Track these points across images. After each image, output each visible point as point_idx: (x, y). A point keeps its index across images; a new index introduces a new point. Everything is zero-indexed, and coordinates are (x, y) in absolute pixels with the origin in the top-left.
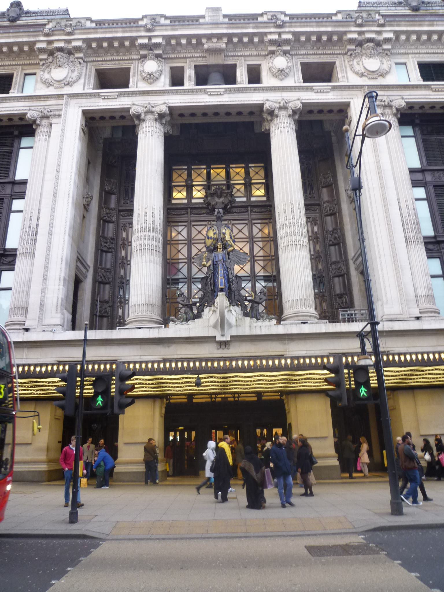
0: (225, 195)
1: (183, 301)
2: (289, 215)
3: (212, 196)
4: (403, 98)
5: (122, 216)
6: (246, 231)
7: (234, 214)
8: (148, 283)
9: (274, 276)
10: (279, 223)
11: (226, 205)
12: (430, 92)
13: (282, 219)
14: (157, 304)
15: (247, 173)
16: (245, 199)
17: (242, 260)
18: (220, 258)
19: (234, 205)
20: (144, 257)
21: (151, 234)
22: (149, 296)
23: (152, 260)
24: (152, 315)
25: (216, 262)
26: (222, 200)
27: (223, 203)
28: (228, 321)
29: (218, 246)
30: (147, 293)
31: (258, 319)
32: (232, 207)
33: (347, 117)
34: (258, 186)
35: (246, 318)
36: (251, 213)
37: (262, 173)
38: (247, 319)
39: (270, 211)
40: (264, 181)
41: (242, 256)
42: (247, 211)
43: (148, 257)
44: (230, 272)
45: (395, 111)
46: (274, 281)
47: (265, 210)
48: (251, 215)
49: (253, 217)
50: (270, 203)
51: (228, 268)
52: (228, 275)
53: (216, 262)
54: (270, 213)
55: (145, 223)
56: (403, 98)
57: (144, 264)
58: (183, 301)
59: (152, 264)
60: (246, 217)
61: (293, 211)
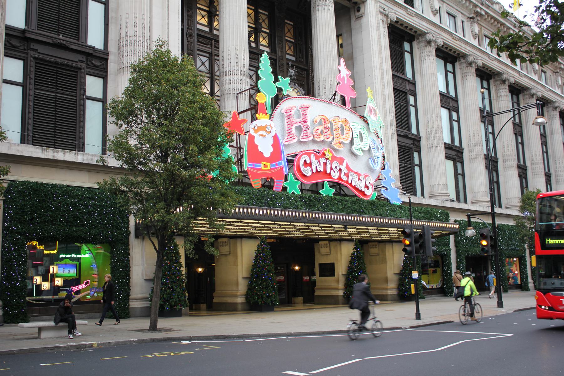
4: (395, 13)
12: (405, 13)
33: (359, 10)
45: (389, 22)
56: (395, 13)
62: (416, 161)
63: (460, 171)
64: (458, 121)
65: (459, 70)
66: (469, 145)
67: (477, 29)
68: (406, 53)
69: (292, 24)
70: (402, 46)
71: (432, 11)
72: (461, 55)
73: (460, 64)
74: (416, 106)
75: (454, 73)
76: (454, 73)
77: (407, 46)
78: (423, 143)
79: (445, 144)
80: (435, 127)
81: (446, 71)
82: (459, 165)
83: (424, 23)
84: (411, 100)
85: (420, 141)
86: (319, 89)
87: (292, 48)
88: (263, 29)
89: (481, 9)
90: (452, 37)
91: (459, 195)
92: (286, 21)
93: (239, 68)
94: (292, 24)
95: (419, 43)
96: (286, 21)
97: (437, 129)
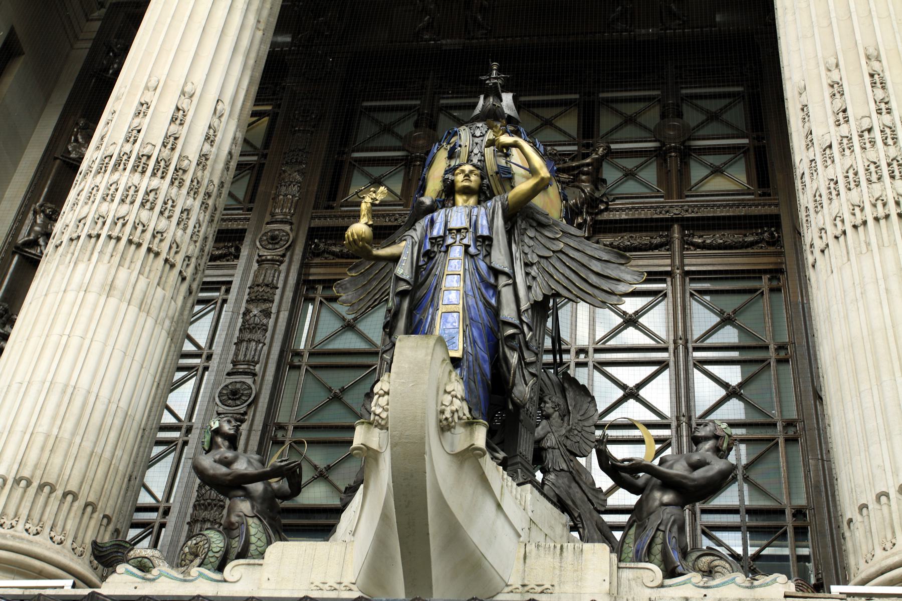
2: (860, 102)
6: (657, 320)
8: (61, 379)
9: (799, 513)
10: (810, 145)
13: (824, 128)
14: (88, 494)
17: (593, 279)
19: (606, 216)
20: (81, 267)
21: (145, 182)
22: (52, 445)
23: (120, 283)
24: (43, 539)
28: (455, 534)
30: (43, 427)
31: (671, 572)
35: (587, 546)
36: (683, 249)
37: (737, 115)
38: (598, 555)
39: (775, 242)
40: (746, 141)
41: (597, 266)
42: (666, 244)
43: (102, 268)
44: (507, 294)
46: (801, 533)
47: (750, 239)
48: (682, 257)
49: (694, 264)
50: (773, 210)
51: (496, 273)
52: (494, 312)
53: (434, 241)
54: (771, 249)
57: (70, 296)
59: (113, 301)
60: (662, 264)
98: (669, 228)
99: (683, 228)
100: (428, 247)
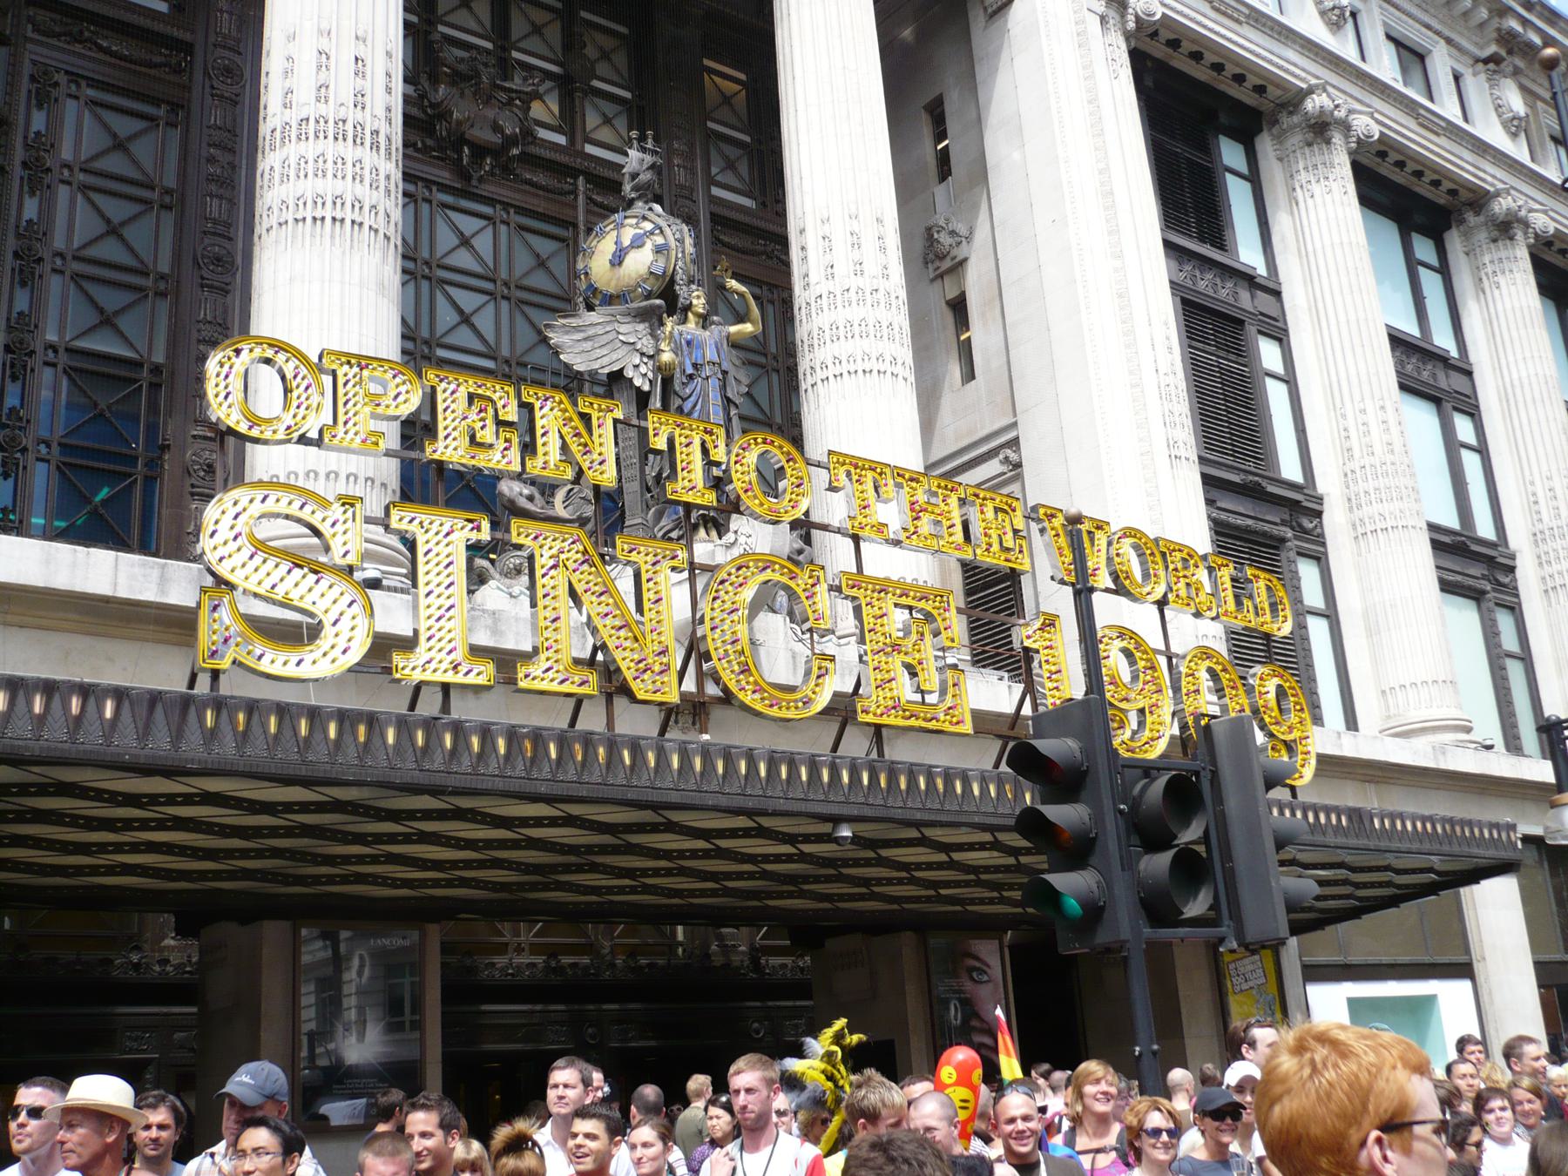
0: (503, 96)
1: (531, 498)
3: (453, 84)
5: (36, 30)
7: (527, 188)
11: (511, 141)
15: (571, 43)
16: (561, 140)
18: (711, 354)
19: (533, 150)
25: (695, 366)
26: (490, 113)
27: (497, 128)
29: (695, 302)
32: (526, 158)
34: (610, 108)
45: (1131, 25)
55: (359, 105)
58: (531, 498)
61: (883, 249)
62: (1312, 595)
63: (1510, 642)
64: (1482, 450)
65: (1462, 256)
66: (1537, 538)
67: (1516, 103)
68: (1231, 180)
69: (743, 77)
70: (1207, 149)
71: (1323, 13)
72: (1464, 195)
73: (1466, 236)
74: (1290, 380)
75: (1444, 270)
76: (1444, 270)
77: (1231, 154)
78: (1335, 522)
79: (1432, 527)
80: (1378, 449)
81: (1412, 265)
82: (1505, 622)
83: (1291, 54)
84: (1269, 354)
85: (1319, 514)
86: (805, 259)
87: (743, 168)
88: (596, 83)
89: (1525, 22)
90: (1417, 117)
91: (1510, 703)
92: (706, 62)
93: (329, 110)
94: (743, 77)
95: (1279, 139)
96: (706, 62)
97: (1389, 458)
98: (576, 178)
99: (588, 181)
100: (690, 370)
